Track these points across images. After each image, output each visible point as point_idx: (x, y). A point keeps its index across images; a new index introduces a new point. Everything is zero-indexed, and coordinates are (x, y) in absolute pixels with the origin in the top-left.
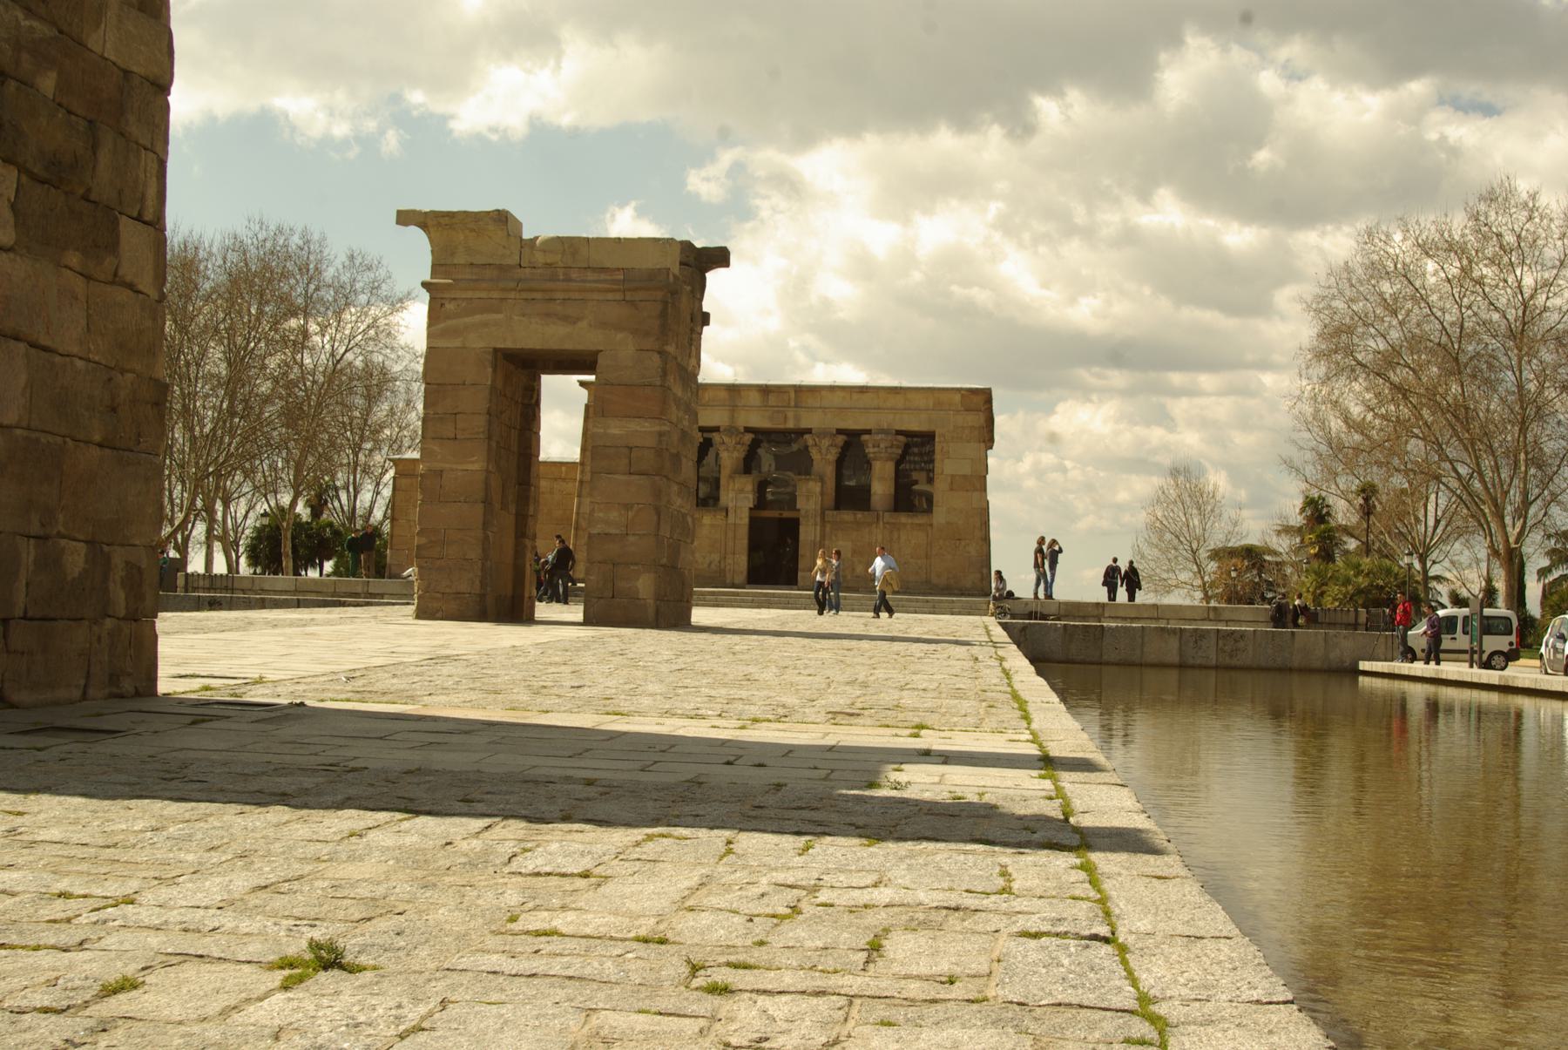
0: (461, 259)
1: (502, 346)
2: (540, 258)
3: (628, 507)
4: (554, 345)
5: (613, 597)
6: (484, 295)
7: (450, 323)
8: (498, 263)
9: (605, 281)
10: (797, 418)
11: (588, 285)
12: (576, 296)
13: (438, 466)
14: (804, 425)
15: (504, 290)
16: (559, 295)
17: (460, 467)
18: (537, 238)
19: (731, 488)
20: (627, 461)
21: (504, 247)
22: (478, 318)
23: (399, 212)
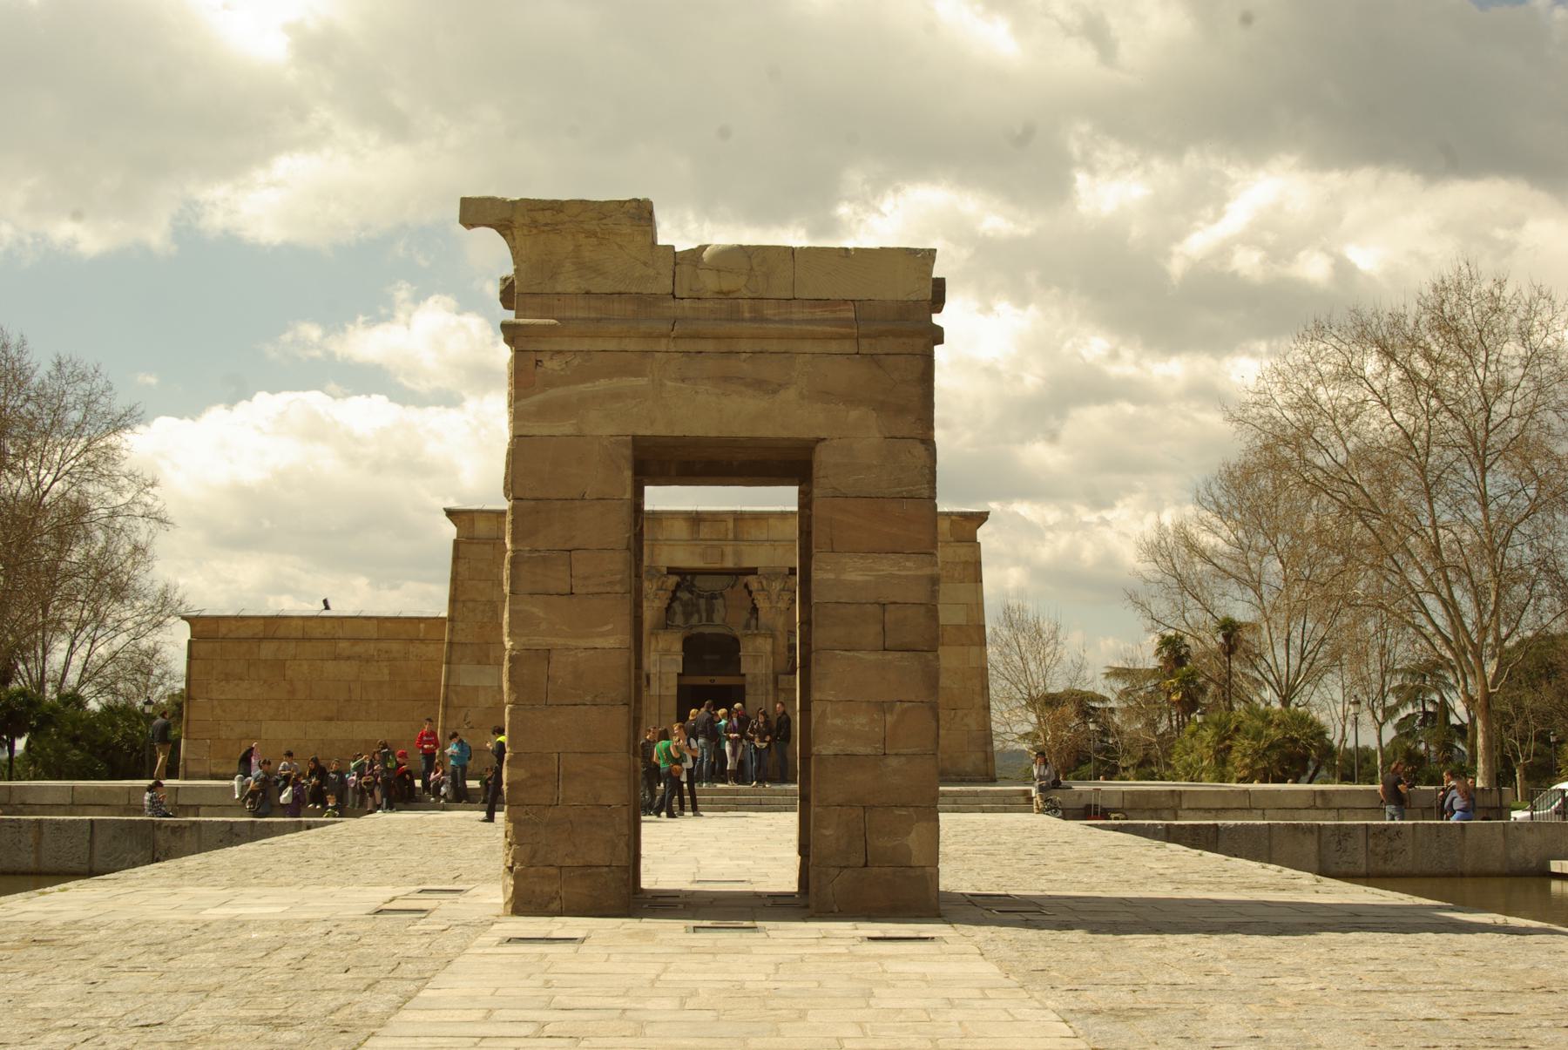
0: (569, 283)
1: (648, 433)
2: (710, 283)
3: (883, 707)
4: (739, 429)
5: (866, 865)
6: (612, 345)
7: (553, 393)
8: (634, 290)
9: (824, 321)
10: (737, 554)
11: (796, 327)
12: (774, 346)
13: (540, 641)
14: (747, 563)
15: (648, 336)
16: (745, 345)
17: (583, 643)
18: (703, 248)
19: (653, 647)
20: (879, 628)
21: (645, 264)
22: (602, 384)
23: (466, 203)
